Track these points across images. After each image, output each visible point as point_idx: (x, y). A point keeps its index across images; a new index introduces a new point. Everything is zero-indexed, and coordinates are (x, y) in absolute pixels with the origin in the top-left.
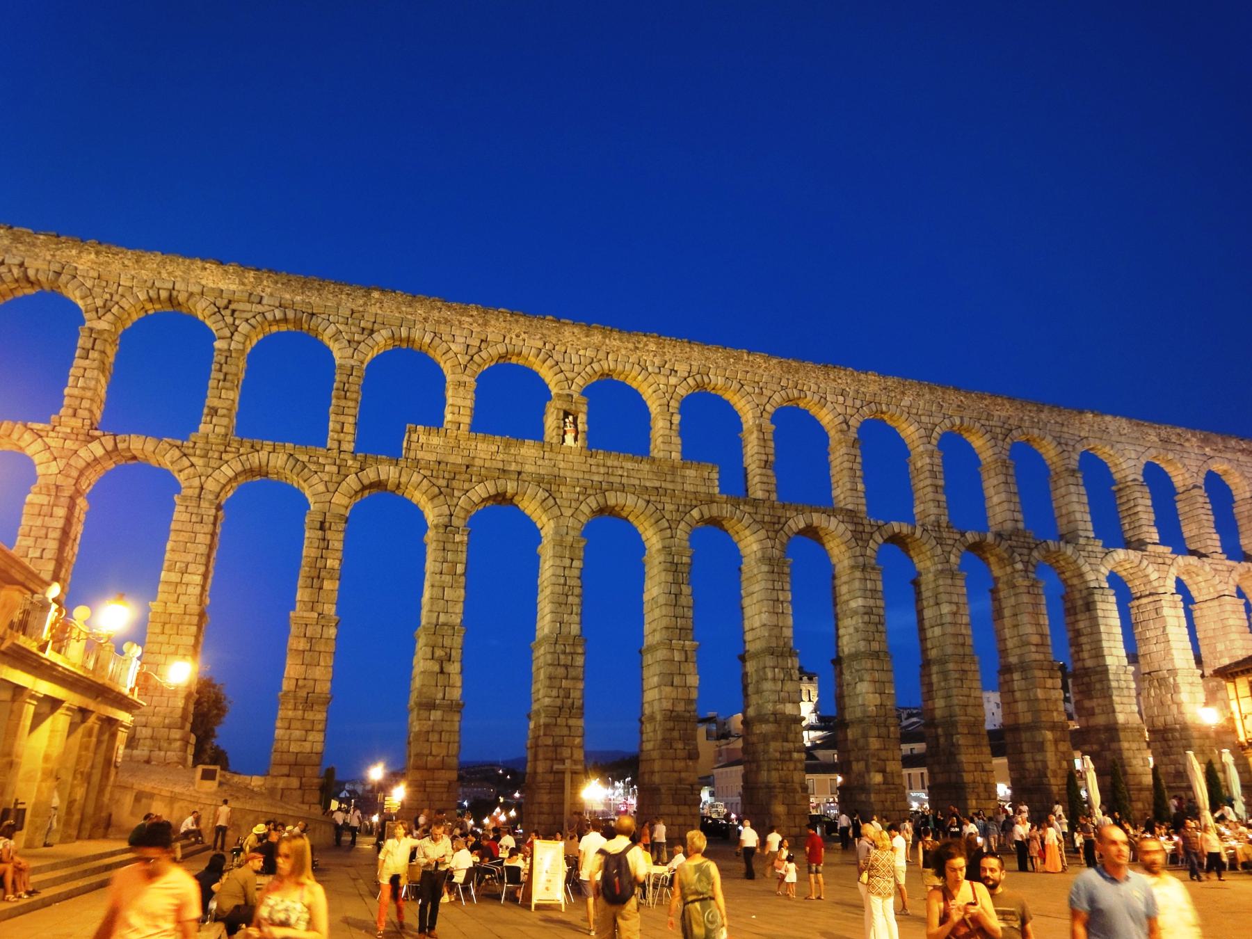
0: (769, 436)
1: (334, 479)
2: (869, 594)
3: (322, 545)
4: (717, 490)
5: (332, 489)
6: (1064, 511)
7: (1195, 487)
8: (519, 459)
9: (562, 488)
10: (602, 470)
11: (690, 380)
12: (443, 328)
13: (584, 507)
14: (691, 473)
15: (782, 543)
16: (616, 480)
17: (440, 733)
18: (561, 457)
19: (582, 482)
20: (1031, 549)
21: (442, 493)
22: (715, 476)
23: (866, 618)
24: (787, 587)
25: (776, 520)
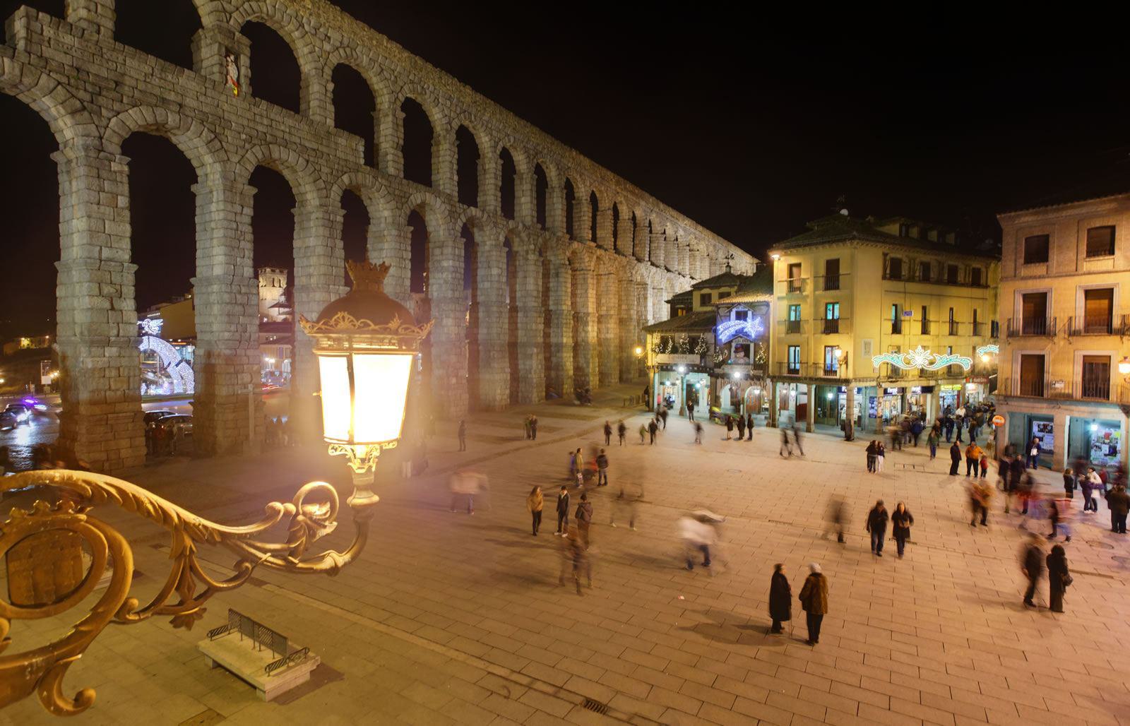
0: (401, 123)
2: (456, 258)
4: (362, 161)
7: (609, 209)
8: (178, 88)
9: (227, 132)
10: (265, 121)
11: (341, 51)
13: (249, 155)
16: (280, 134)
18: (223, 98)
19: (247, 130)
20: (538, 236)
22: (362, 149)
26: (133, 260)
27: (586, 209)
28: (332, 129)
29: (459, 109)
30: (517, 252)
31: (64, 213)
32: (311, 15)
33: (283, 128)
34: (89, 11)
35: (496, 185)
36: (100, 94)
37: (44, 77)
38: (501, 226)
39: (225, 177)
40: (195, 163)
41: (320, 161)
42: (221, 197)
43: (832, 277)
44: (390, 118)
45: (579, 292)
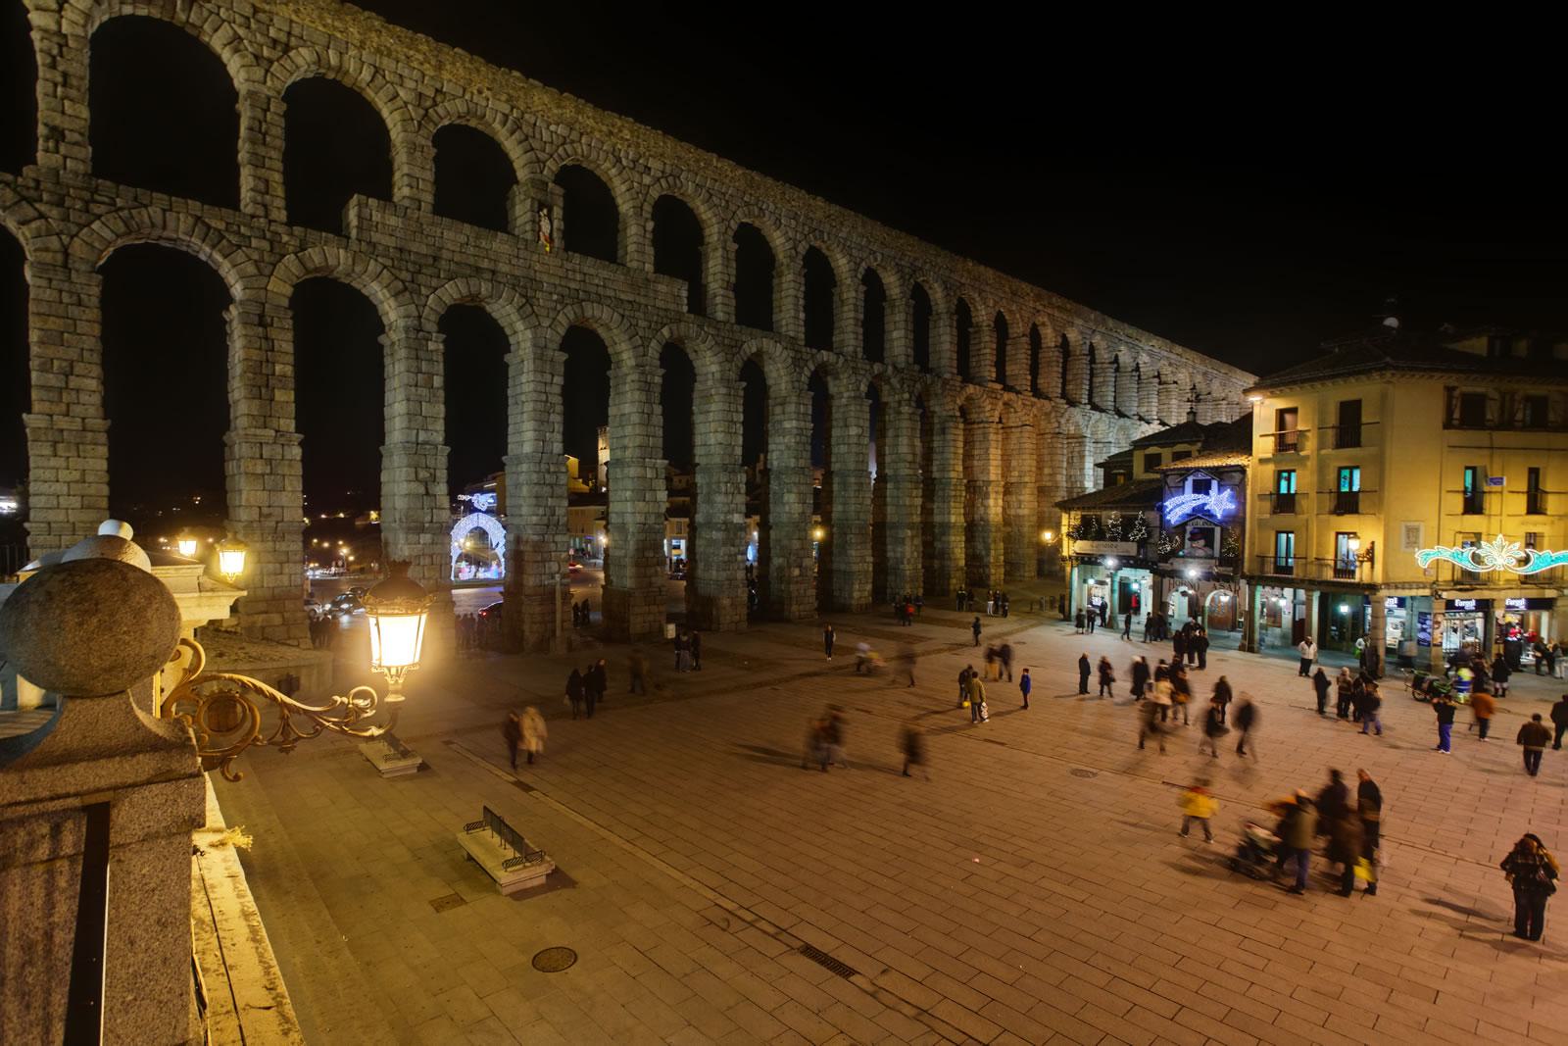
0: (732, 256)
1: (266, 257)
3: (264, 346)
4: (685, 309)
5: (266, 272)
7: (1024, 335)
9: (539, 295)
10: (578, 277)
11: (663, 181)
12: (387, 63)
13: (560, 317)
14: (662, 288)
15: (736, 366)
16: (593, 289)
17: (431, 556)
18: (535, 257)
19: (559, 289)
20: (915, 382)
21: (406, 290)
22: (684, 294)
23: (798, 438)
24: (741, 409)
25: (733, 343)
26: (446, 442)
27: (987, 339)
28: (652, 276)
29: (807, 228)
30: (886, 404)
31: (389, 397)
32: (629, 146)
33: (596, 281)
34: (412, 188)
35: (856, 319)
36: (419, 272)
37: (372, 261)
39: (535, 346)
40: (508, 331)
41: (637, 314)
42: (532, 367)
43: (1348, 429)
44: (720, 252)
45: (976, 452)
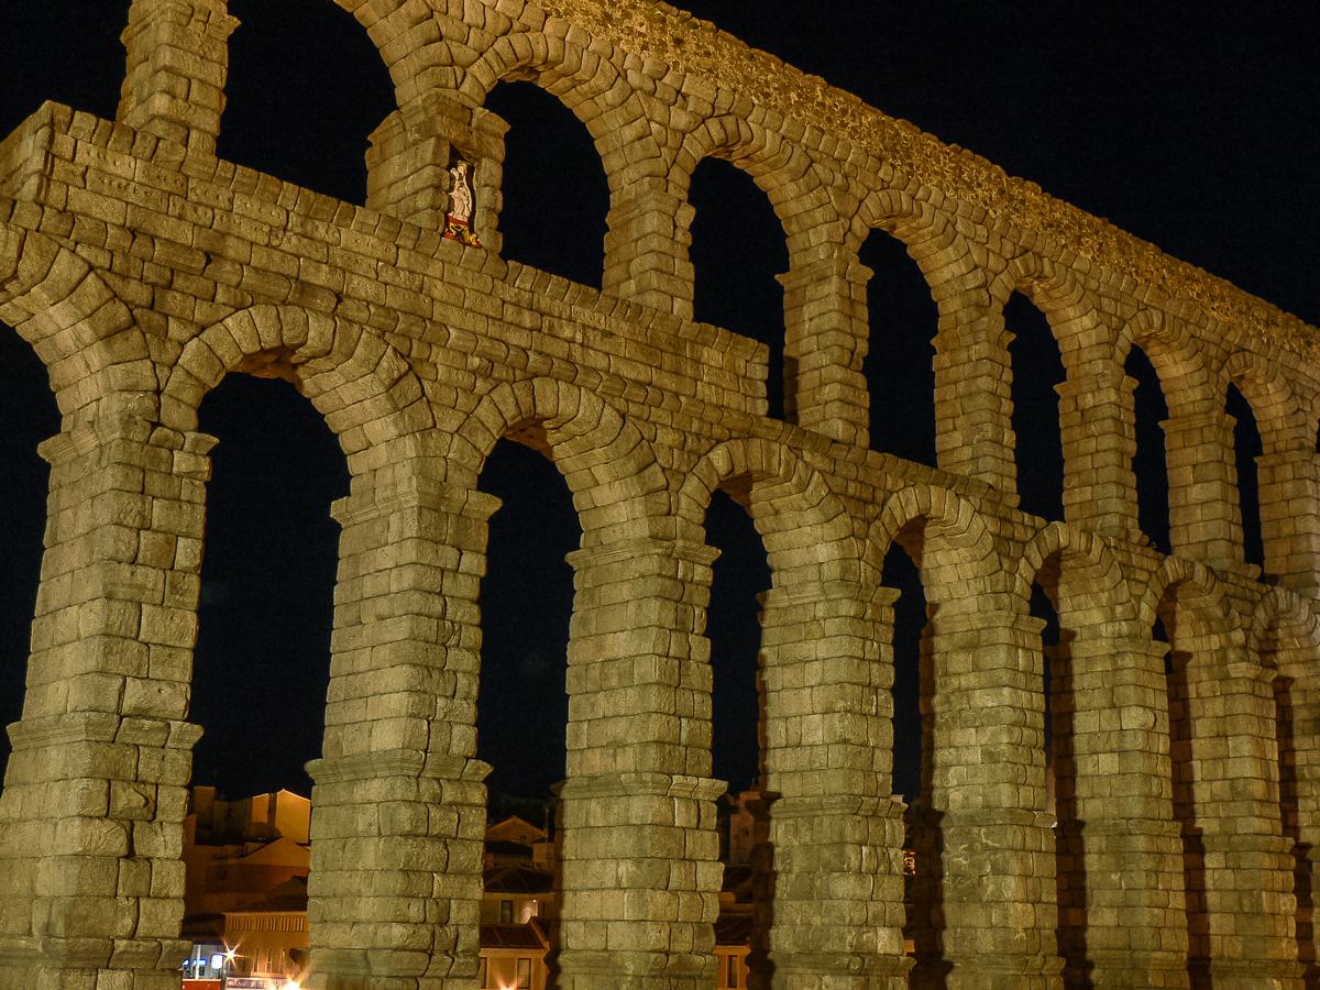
0: (861, 294)
6: (1287, 530)
8: (337, 256)
9: (438, 356)
10: (527, 319)
11: (713, 125)
13: (484, 411)
14: (712, 356)
15: (875, 548)
19: (485, 344)
21: (136, 323)
25: (867, 495)
26: (194, 713)
28: (689, 327)
29: (1008, 247)
31: (51, 590)
32: (645, 47)
33: (567, 333)
34: (174, 97)
35: (1122, 453)
36: (169, 286)
37: (64, 255)
38: (1143, 576)
39: (423, 473)
40: (347, 443)
42: (412, 529)
44: (833, 286)
